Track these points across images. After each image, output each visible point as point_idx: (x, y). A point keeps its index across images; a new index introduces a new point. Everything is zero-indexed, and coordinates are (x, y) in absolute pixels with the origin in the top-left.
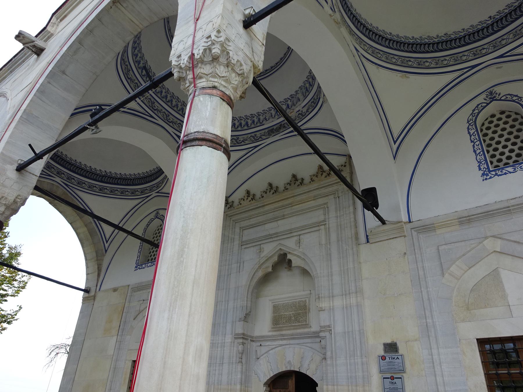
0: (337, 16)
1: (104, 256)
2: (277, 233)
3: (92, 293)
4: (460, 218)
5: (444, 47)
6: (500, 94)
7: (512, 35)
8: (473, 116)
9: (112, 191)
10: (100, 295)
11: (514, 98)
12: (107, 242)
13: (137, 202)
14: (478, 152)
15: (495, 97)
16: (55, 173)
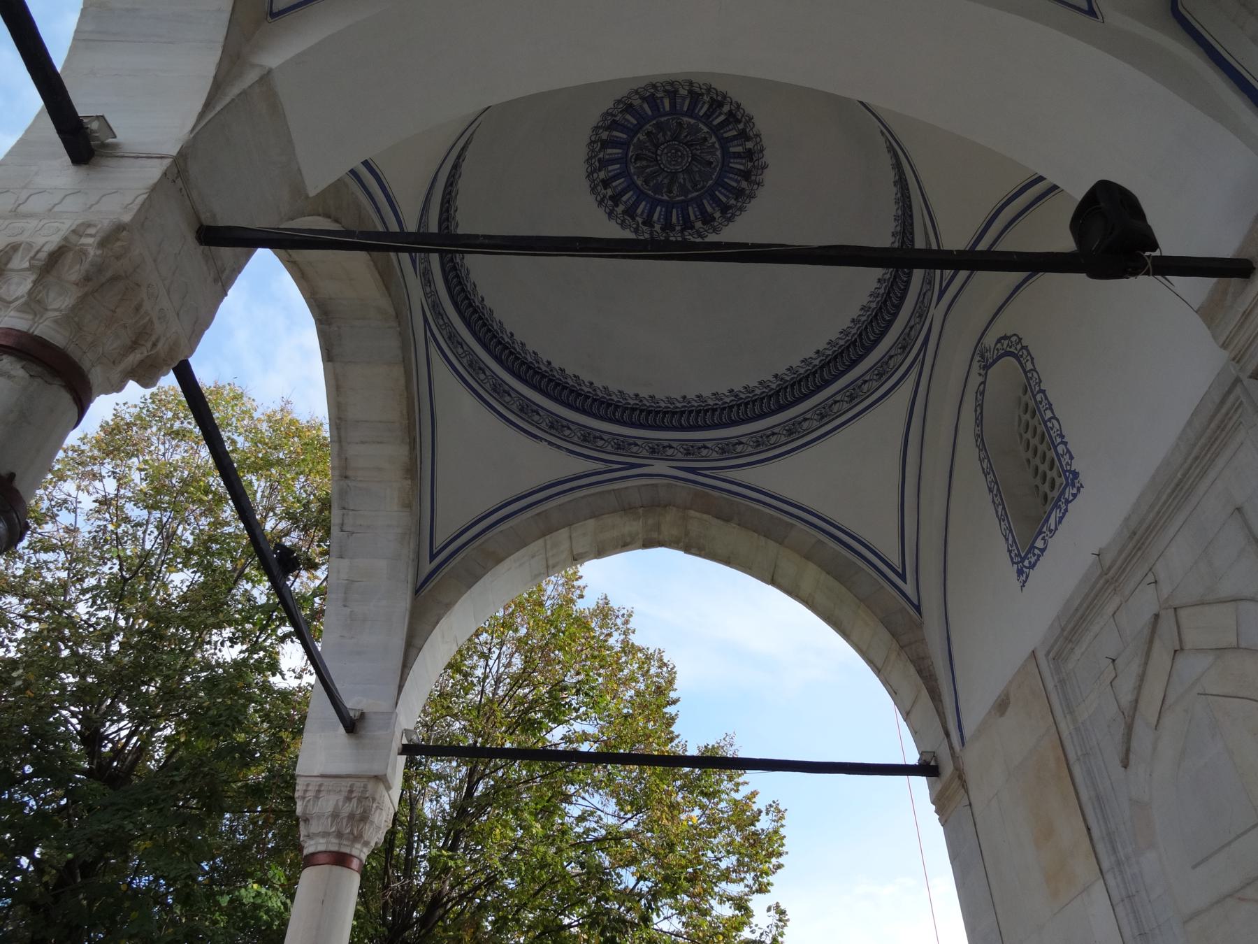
1: (920, 626)
3: (948, 769)
9: (823, 414)
10: (971, 758)
12: (903, 577)
16: (645, 453)
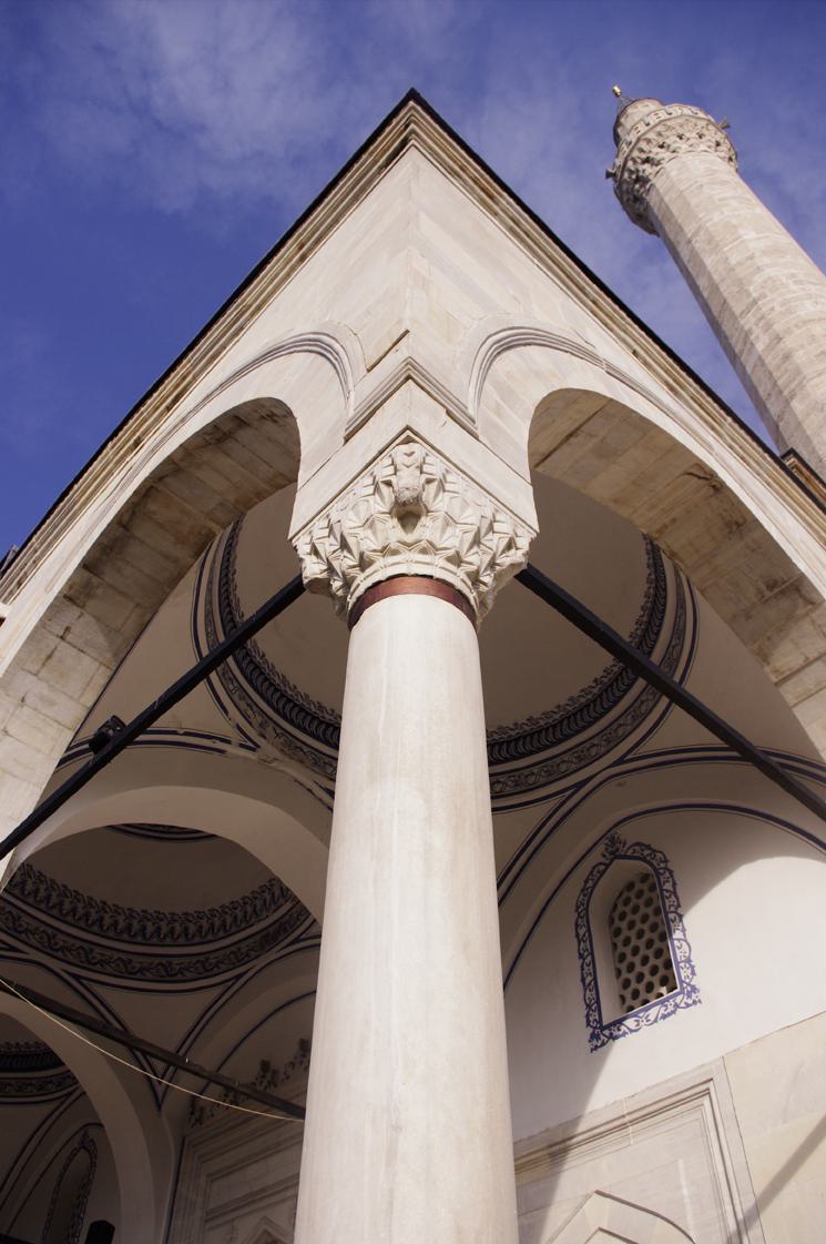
0: (268, 748)
2: (263, 1190)
4: (551, 1146)
5: (529, 747)
6: (625, 843)
7: (630, 717)
8: (585, 895)
11: (646, 852)
13: (52, 1106)
14: (587, 981)
15: (617, 850)
